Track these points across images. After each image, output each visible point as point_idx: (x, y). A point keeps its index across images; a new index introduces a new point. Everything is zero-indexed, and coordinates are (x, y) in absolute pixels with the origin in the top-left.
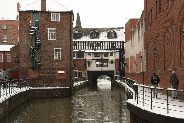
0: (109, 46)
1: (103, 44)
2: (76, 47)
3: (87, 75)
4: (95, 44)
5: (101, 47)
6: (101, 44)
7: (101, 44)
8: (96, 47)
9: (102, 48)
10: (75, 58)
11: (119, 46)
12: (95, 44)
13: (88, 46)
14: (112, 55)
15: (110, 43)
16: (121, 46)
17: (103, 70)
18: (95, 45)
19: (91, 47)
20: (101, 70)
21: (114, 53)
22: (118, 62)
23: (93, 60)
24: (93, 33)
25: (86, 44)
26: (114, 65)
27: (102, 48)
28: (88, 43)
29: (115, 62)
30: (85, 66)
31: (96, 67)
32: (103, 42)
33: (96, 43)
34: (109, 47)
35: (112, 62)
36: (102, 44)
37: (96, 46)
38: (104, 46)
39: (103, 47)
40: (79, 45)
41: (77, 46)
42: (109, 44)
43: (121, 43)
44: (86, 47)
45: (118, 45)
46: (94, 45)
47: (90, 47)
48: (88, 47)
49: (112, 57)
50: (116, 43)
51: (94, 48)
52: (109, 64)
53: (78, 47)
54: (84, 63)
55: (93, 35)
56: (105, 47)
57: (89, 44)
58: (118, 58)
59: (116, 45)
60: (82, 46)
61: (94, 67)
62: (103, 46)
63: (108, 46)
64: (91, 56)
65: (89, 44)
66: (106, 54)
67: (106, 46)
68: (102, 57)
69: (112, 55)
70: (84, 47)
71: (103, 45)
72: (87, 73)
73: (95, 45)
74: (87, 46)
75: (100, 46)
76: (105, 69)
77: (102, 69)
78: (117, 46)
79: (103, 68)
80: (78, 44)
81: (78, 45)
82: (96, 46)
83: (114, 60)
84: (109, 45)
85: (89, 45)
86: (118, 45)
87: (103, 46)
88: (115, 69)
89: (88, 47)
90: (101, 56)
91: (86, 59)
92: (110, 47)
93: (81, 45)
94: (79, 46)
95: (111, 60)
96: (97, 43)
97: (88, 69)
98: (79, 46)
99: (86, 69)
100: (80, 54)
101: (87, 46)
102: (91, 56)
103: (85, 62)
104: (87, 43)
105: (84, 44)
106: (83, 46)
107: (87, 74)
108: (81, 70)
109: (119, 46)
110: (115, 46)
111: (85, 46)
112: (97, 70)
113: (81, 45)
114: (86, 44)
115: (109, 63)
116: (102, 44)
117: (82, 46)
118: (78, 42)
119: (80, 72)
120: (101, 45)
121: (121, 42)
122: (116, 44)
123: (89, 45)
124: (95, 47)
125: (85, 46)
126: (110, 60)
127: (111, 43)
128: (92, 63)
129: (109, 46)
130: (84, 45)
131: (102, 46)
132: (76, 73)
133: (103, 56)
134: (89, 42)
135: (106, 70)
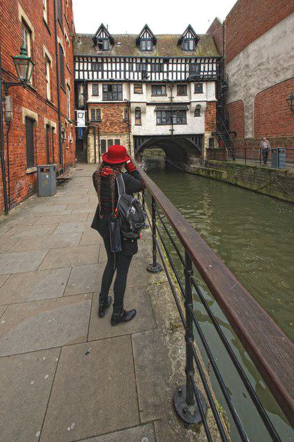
0: (185, 72)
1: (170, 66)
2: (100, 73)
3: (132, 149)
4: (149, 66)
5: (165, 74)
6: (165, 66)
7: (165, 66)
8: (153, 74)
9: (168, 76)
10: (99, 99)
11: (208, 71)
12: (149, 66)
13: (132, 71)
14: (199, 90)
15: (185, 64)
16: (212, 71)
17: (175, 133)
18: (149, 69)
19: (140, 74)
20: (169, 133)
21: (204, 85)
22: (214, 111)
23: (148, 104)
24: (144, 40)
25: (127, 65)
26: (202, 118)
27: (168, 76)
28: (133, 63)
29: (207, 110)
30: (127, 121)
31: (157, 125)
32: (171, 61)
33: (151, 63)
34: (183, 74)
35: (197, 112)
36: (168, 68)
37: (151, 72)
38: (172, 71)
39: (170, 74)
40: (110, 69)
41: (103, 71)
42: (183, 66)
43: (215, 65)
44: (127, 73)
45: (206, 69)
46: (147, 67)
47: (136, 74)
48: (132, 73)
49: (199, 95)
50: (200, 64)
51: (147, 78)
52: (190, 117)
53: (105, 73)
54: (123, 114)
55: (143, 43)
56: (175, 74)
57: (134, 65)
58: (213, 98)
59: (202, 69)
60: (116, 71)
61: (150, 125)
62: (170, 71)
63: (181, 72)
64: (142, 93)
65: (134, 65)
66: (182, 87)
67: (177, 72)
68: (172, 98)
69: (199, 90)
70: (122, 73)
71: (170, 69)
72: (132, 141)
73: (149, 69)
74: (129, 71)
75: (163, 72)
76: (180, 130)
77: (172, 130)
78: (204, 71)
79: (175, 127)
80: (105, 65)
81: (105, 68)
82: (151, 72)
83: (204, 105)
84: (183, 70)
85: (134, 69)
86: (206, 69)
87: (170, 71)
88: (206, 130)
89: (132, 73)
90: (169, 94)
91: (128, 104)
92: (188, 74)
93: (114, 69)
94: (108, 71)
95: (198, 106)
96: (155, 63)
97: (136, 130)
98: (108, 71)
99: (130, 132)
100: (112, 87)
101: (129, 71)
102: (142, 93)
103: (127, 111)
104: (129, 63)
105: (122, 65)
106: (120, 71)
107: (132, 144)
108: (117, 135)
109: (208, 71)
110: (200, 71)
111: (125, 71)
112: (160, 133)
113: (114, 69)
114: (127, 65)
115: (191, 112)
116: (168, 68)
117: (116, 71)
118: (105, 61)
119: (114, 138)
120: (165, 69)
121: (215, 61)
122: (202, 66)
123: (134, 69)
124: (149, 74)
125: (125, 71)
126: (194, 105)
127: (190, 64)
128: (145, 113)
129: (185, 72)
130: (122, 69)
131: (167, 72)
132: (104, 141)
133: (175, 93)
134: (134, 61)
135: (181, 133)
